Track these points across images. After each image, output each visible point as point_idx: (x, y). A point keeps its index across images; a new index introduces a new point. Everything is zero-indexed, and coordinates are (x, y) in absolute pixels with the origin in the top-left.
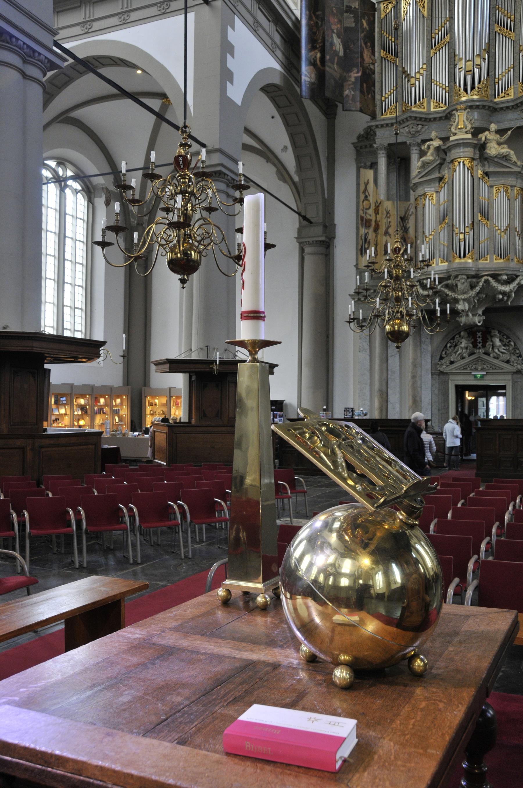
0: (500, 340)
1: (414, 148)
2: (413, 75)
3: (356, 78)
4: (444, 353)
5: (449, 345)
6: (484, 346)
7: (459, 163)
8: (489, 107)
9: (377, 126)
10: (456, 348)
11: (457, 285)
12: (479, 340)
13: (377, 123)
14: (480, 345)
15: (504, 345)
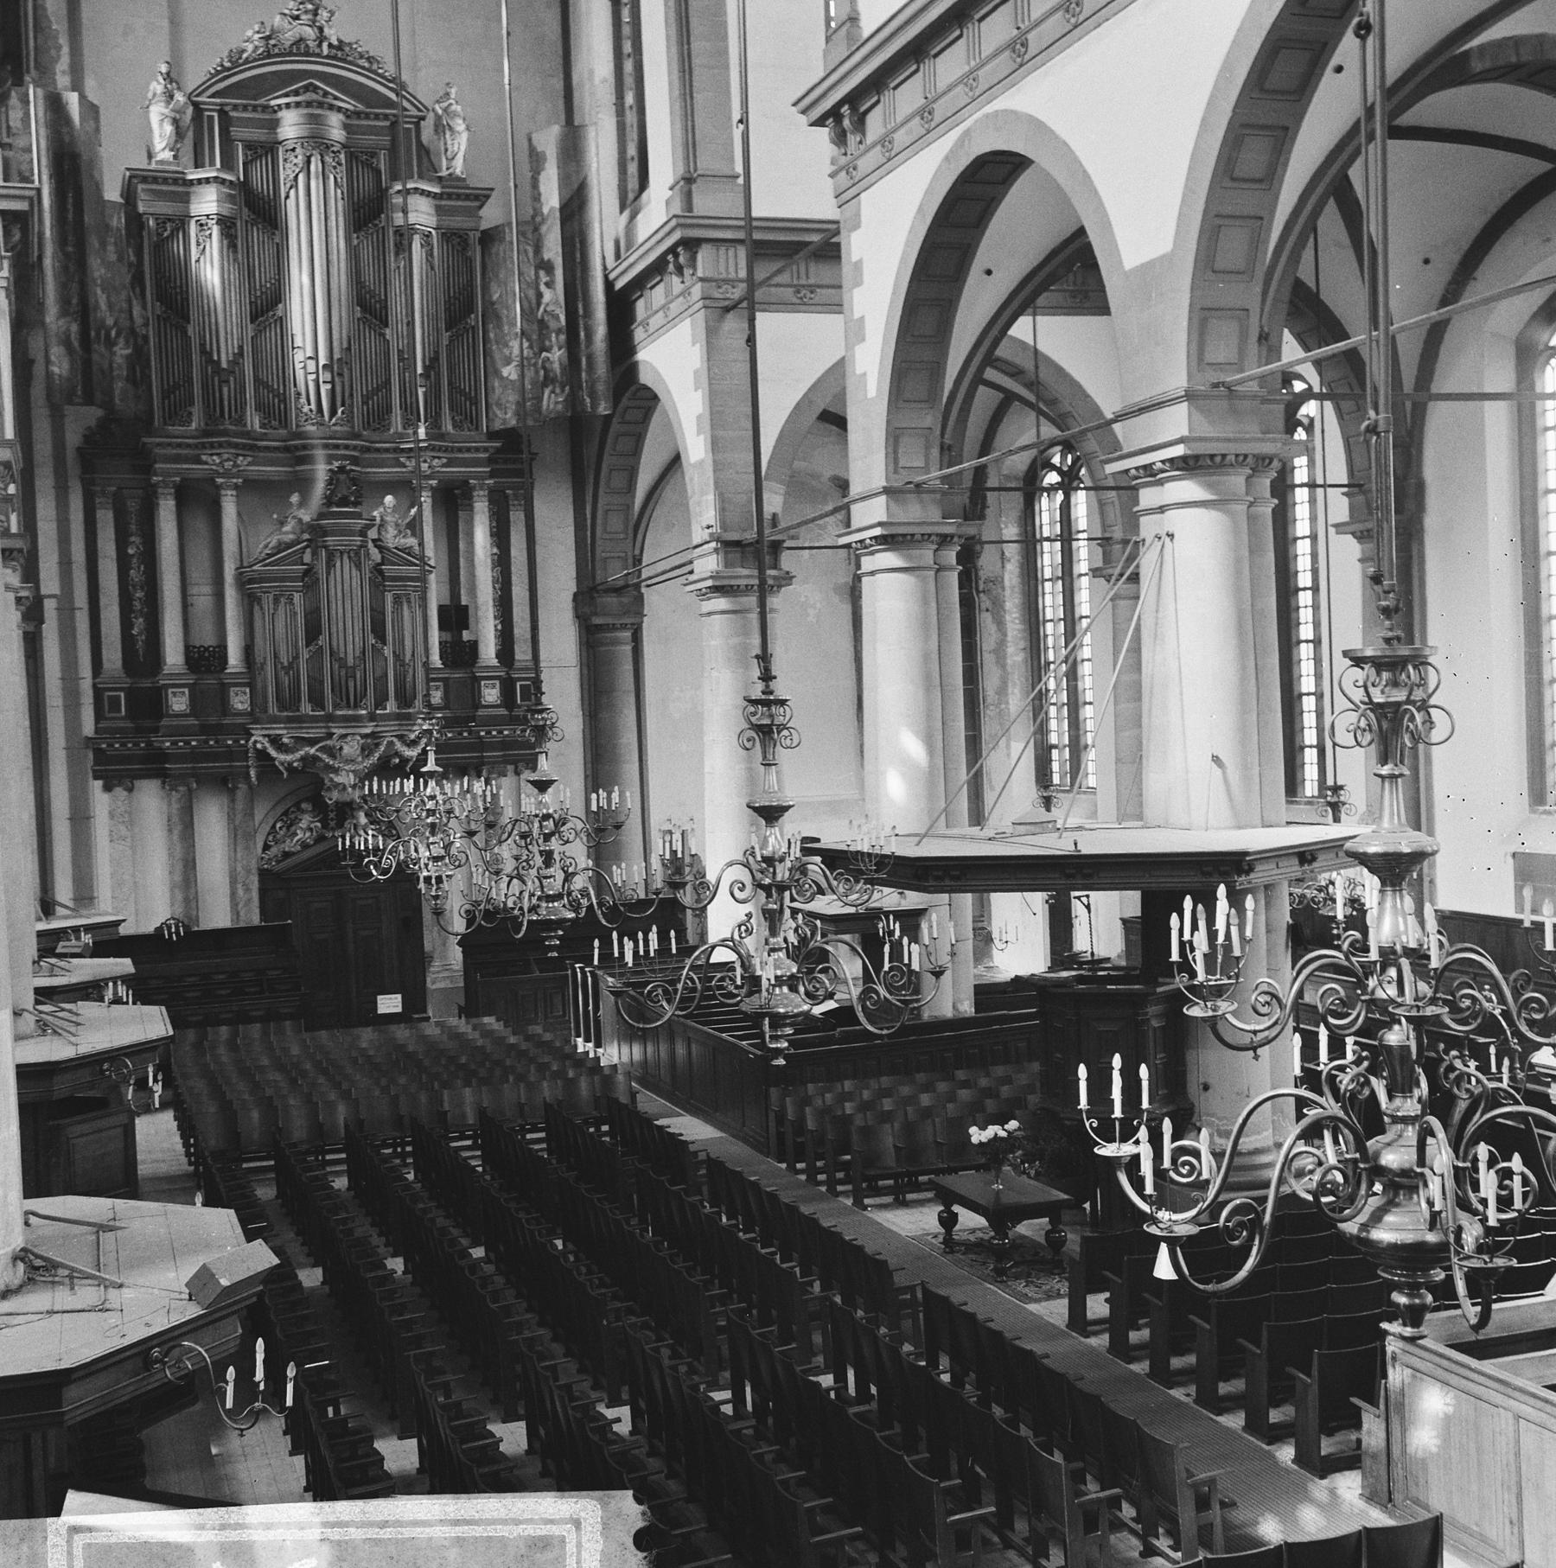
0: (366, 815)
1: (229, 493)
2: (224, 365)
3: (128, 357)
4: (271, 838)
5: (278, 825)
6: (340, 825)
7: (341, 553)
8: (362, 446)
9: (159, 444)
10: (293, 828)
11: (341, 748)
12: (332, 815)
13: (158, 440)
14: (332, 824)
15: (372, 823)
